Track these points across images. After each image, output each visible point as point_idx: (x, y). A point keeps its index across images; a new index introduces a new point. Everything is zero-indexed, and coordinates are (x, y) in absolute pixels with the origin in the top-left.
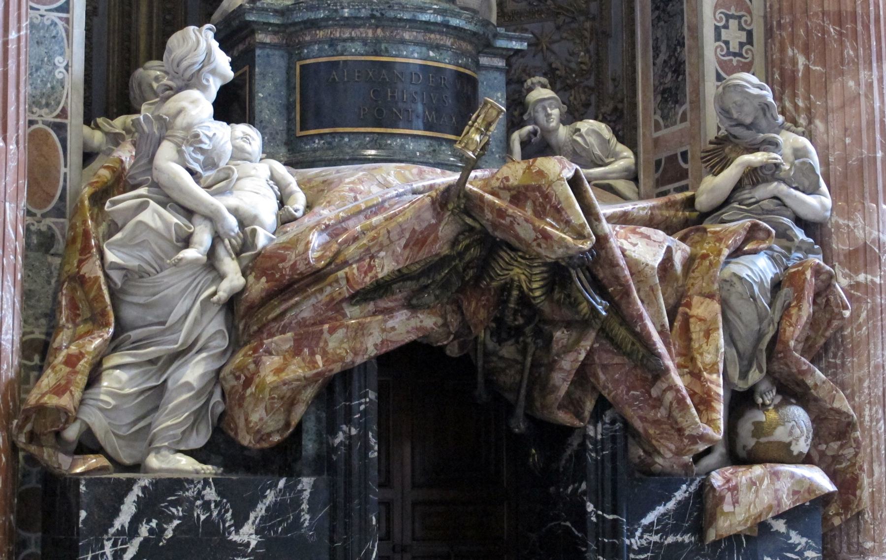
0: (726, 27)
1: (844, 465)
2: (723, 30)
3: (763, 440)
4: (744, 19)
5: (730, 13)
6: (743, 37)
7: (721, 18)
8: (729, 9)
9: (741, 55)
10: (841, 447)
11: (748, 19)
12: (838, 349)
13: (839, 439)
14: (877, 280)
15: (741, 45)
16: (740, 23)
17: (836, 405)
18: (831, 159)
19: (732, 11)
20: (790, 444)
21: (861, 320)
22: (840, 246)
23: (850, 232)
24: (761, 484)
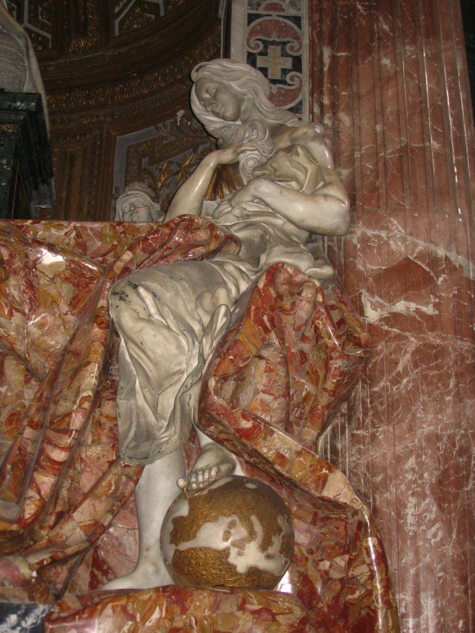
0: (264, 54)
1: (357, 594)
2: (259, 58)
3: (184, 546)
4: (289, 45)
5: (271, 39)
6: (288, 64)
7: (257, 46)
8: (269, 36)
9: (284, 82)
10: (350, 563)
11: (296, 45)
12: (365, 414)
13: (348, 552)
14: (429, 310)
15: (285, 71)
16: (283, 49)
17: (328, 493)
18: (357, 155)
19: (274, 37)
20: (226, 553)
21: (400, 368)
22: (369, 266)
23: (383, 244)
24: (145, 619)
